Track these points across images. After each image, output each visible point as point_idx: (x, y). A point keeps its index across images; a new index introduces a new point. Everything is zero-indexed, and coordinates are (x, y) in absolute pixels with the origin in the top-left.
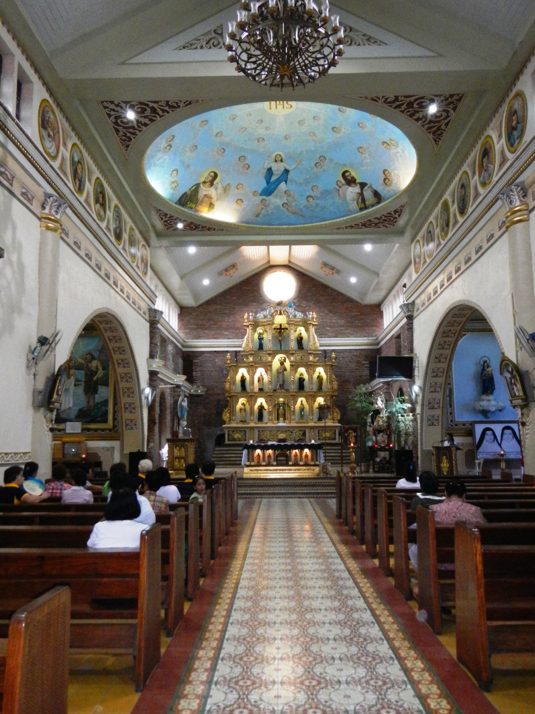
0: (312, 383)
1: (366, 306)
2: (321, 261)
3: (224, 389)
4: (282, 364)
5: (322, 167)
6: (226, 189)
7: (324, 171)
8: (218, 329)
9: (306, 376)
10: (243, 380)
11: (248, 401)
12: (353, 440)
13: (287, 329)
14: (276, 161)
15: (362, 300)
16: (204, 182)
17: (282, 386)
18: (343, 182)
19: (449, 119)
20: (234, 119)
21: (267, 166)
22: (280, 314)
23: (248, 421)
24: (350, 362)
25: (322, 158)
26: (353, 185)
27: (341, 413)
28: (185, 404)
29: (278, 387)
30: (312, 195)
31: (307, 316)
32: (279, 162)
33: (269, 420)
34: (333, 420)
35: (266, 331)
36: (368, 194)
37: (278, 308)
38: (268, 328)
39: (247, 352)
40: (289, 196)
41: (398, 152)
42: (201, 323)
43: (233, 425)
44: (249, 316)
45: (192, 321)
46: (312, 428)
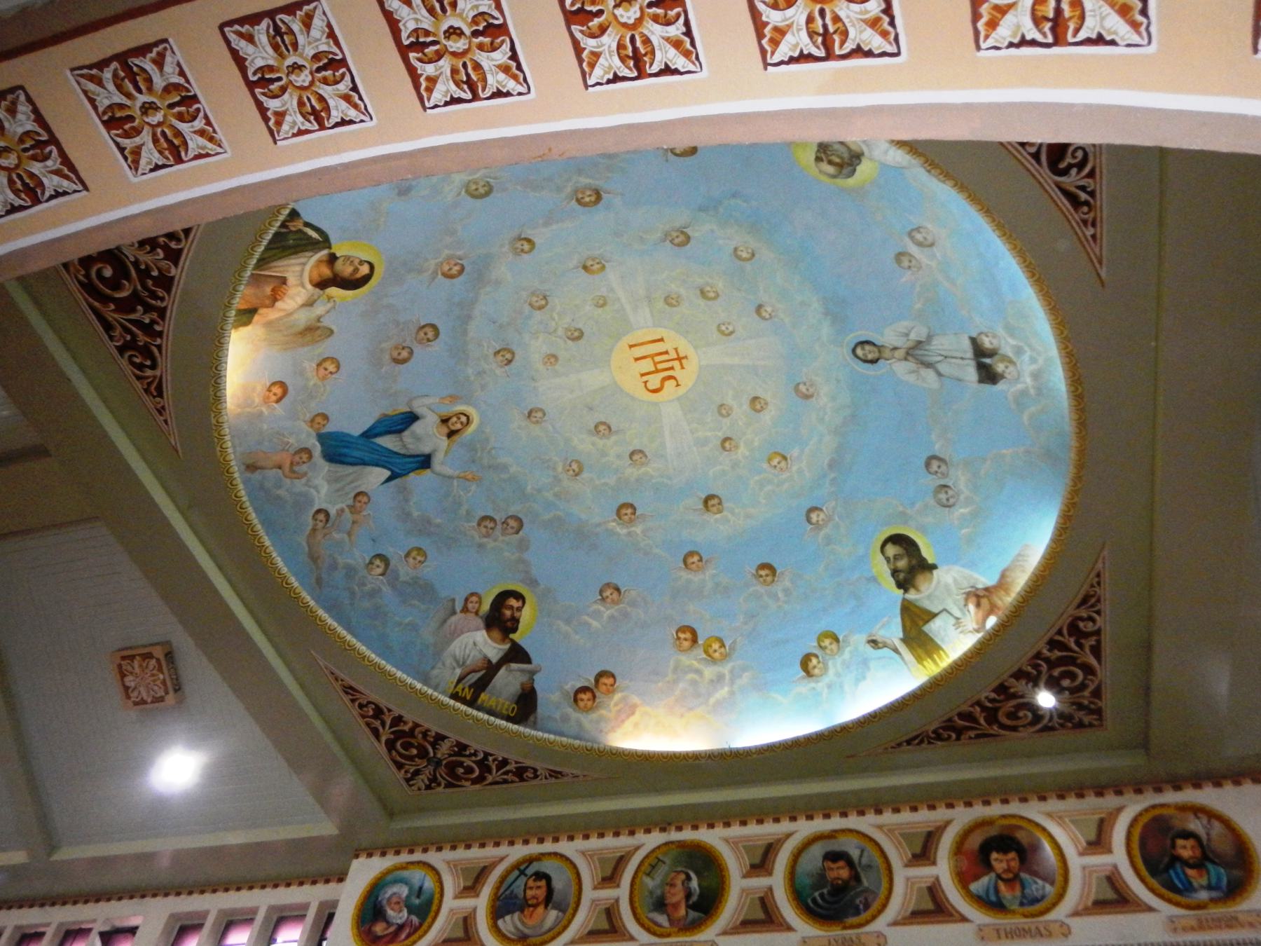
5: (487, 536)
6: (314, 332)
7: (480, 546)
14: (445, 421)
16: (332, 259)
18: (486, 607)
19: (1003, 732)
20: (585, 268)
21: (418, 408)
25: (512, 523)
26: (496, 634)
30: (393, 563)
32: (446, 431)
36: (508, 682)
40: (350, 507)
41: (698, 672)
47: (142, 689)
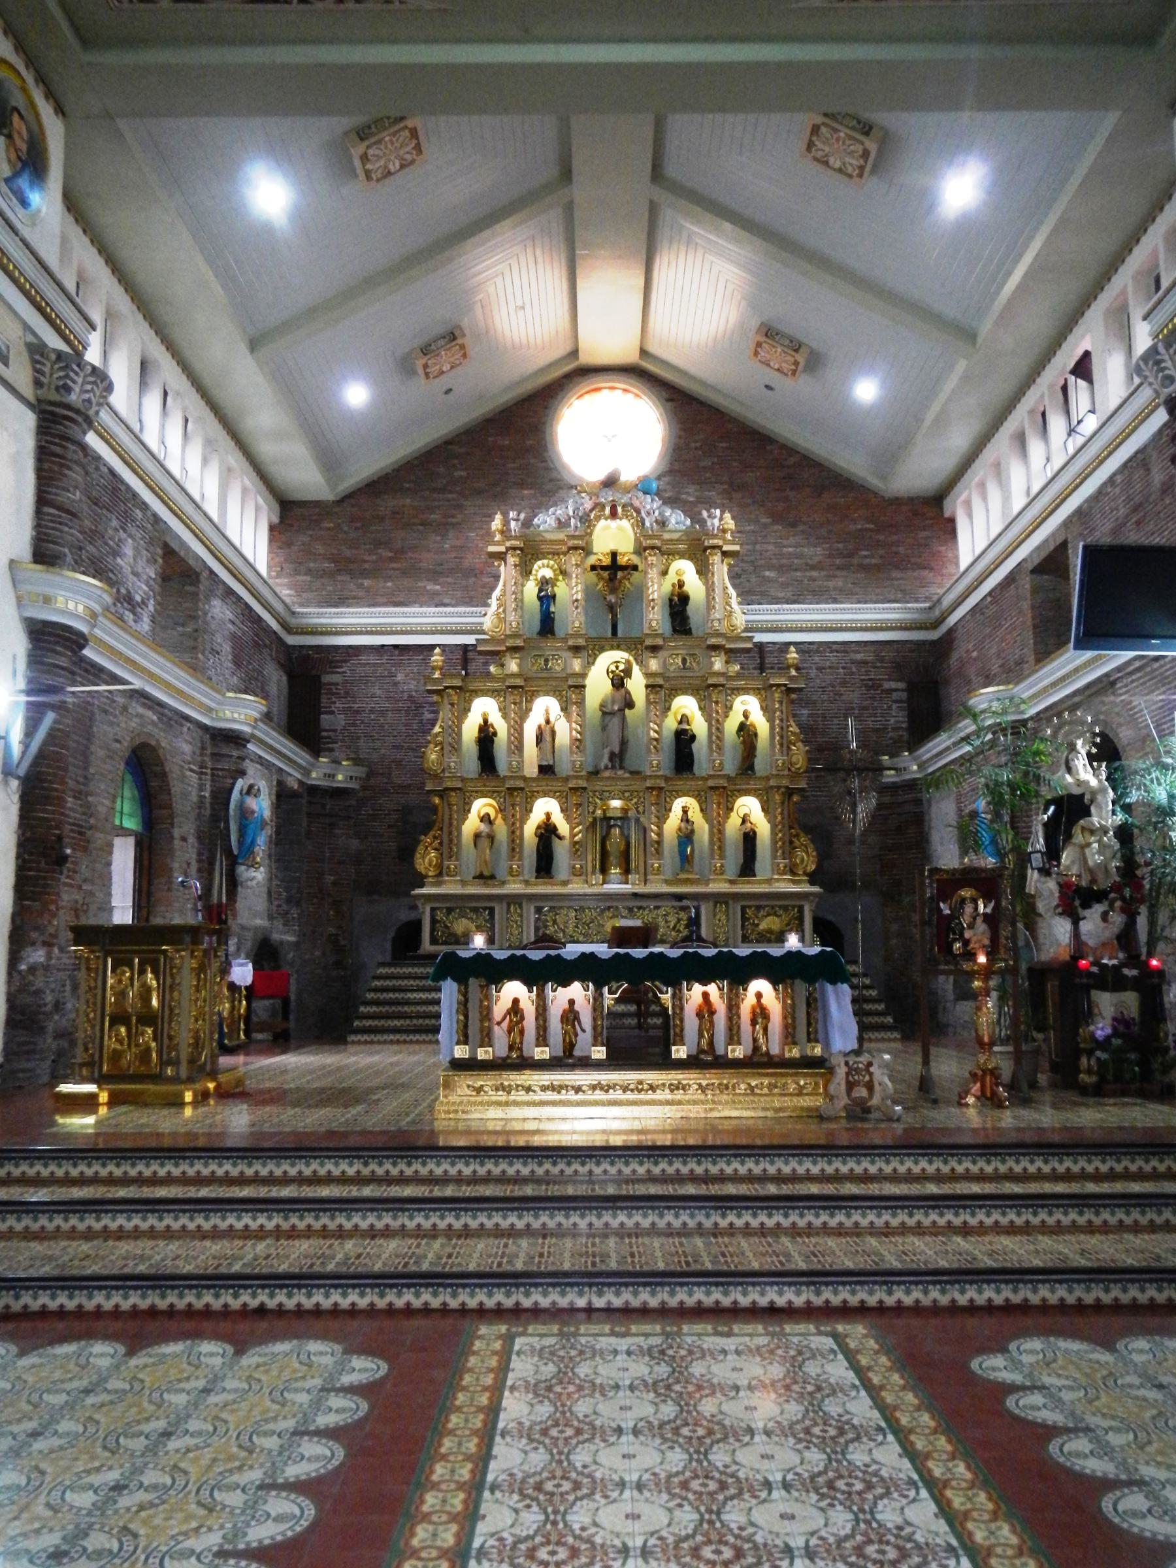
0: (720, 748)
1: (897, 502)
2: (755, 323)
3: (422, 771)
4: (618, 682)
8: (405, 573)
9: (699, 726)
10: (486, 736)
11: (501, 810)
12: (978, 934)
13: (635, 568)
15: (884, 478)
17: (618, 758)
22: (614, 515)
23: (501, 873)
24: (844, 683)
27: (817, 849)
28: (262, 805)
29: (605, 760)
31: (703, 522)
33: (576, 873)
34: (793, 873)
35: (564, 573)
37: (607, 497)
38: (574, 559)
39: (500, 642)
42: (348, 553)
43: (450, 888)
44: (506, 523)
45: (320, 549)
46: (720, 899)
47: (847, 160)
